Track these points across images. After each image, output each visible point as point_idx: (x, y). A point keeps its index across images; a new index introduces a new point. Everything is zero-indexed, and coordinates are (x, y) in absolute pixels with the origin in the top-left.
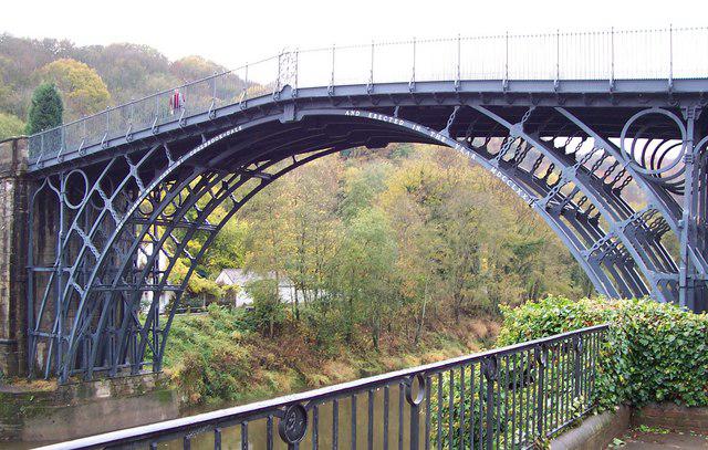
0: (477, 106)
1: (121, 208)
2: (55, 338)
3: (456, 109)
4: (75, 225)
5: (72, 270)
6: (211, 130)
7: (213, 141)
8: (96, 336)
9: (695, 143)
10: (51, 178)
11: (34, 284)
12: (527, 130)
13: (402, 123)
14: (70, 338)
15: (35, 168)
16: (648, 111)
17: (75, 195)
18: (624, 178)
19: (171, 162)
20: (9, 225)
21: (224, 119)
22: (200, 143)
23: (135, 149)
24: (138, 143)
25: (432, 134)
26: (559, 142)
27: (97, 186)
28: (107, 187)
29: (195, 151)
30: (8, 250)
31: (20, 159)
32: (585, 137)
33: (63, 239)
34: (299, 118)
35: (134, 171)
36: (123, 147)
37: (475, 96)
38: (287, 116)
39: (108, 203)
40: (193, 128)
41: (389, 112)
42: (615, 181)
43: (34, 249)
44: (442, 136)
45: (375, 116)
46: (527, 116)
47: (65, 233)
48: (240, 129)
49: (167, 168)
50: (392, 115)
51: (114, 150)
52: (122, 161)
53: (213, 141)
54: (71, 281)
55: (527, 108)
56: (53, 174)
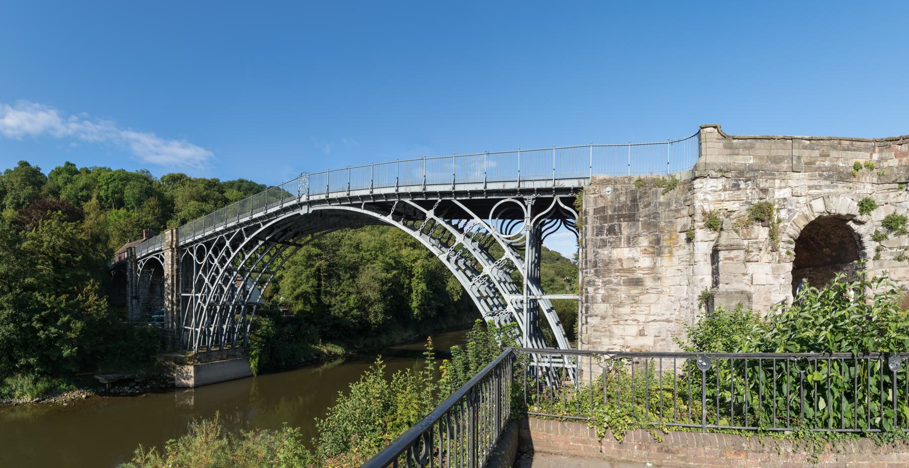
0: (407, 201)
1: (223, 261)
3: (396, 203)
4: (200, 273)
9: (531, 221)
11: (183, 303)
12: (437, 214)
13: (366, 212)
16: (502, 201)
18: (490, 242)
26: (455, 222)
32: (469, 218)
33: (195, 280)
37: (406, 195)
41: (359, 206)
42: (485, 243)
44: (388, 219)
45: (352, 209)
46: (436, 206)
50: (361, 208)
54: (199, 301)
55: (437, 201)
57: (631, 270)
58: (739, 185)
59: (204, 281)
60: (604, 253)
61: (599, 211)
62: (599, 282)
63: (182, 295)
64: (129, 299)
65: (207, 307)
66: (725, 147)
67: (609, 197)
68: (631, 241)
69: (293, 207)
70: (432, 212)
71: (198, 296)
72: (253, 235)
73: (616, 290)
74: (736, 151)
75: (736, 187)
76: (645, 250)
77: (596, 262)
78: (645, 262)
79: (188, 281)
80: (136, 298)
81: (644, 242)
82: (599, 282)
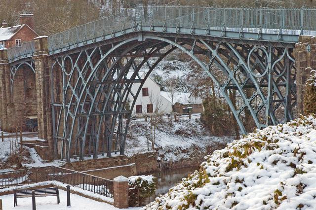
2: (64, 140)
4: (68, 84)
5: (69, 106)
6: (115, 42)
7: (117, 46)
8: (84, 139)
10: (58, 58)
14: (69, 140)
19: (102, 56)
20: (41, 84)
21: (116, 38)
22: (111, 48)
23: (90, 49)
25: (187, 52)
30: (42, 95)
31: (44, 49)
33: (64, 91)
34: (144, 40)
35: (89, 59)
36: (82, 47)
38: (140, 39)
39: (80, 73)
43: (54, 95)
47: (65, 88)
48: (125, 42)
49: (100, 59)
50: (174, 42)
51: (79, 48)
53: (117, 46)
56: (58, 57)
63: (55, 105)
65: (75, 118)
67: (309, 53)
69: (133, 34)
70: (215, 51)
71: (67, 107)
72: (107, 54)
79: (59, 90)
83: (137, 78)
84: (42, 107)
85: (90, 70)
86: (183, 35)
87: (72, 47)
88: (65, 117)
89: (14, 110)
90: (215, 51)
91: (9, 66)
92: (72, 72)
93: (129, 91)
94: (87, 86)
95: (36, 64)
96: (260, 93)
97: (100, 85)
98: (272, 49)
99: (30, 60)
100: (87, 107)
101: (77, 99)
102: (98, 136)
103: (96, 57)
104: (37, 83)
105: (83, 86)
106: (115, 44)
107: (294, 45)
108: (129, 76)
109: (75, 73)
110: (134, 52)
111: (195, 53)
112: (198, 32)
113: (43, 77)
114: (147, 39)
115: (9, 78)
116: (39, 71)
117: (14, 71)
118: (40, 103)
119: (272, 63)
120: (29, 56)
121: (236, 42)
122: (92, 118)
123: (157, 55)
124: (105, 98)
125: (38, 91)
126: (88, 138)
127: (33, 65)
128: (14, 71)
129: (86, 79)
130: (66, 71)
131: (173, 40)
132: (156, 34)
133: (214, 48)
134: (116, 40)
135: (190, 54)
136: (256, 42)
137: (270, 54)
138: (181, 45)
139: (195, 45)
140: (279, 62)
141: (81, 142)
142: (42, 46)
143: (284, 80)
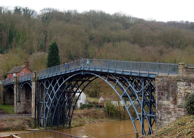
4: (47, 93)
5: (47, 103)
8: (53, 118)
14: (46, 118)
15: (39, 79)
17: (47, 85)
21: (72, 73)
23: (58, 77)
24: (58, 76)
25: (105, 80)
27: (51, 84)
28: (53, 84)
29: (68, 79)
35: (57, 81)
38: (82, 73)
39: (53, 88)
40: (67, 74)
47: (45, 94)
50: (99, 75)
52: (55, 78)
56: (43, 80)
57: (167, 109)
58: (190, 84)
59: (48, 96)
60: (160, 101)
61: (158, 87)
62: (159, 111)
64: (15, 102)
66: (186, 71)
68: (168, 98)
69: (79, 71)
72: (66, 80)
73: (164, 115)
74: (190, 73)
75: (190, 85)
76: (172, 102)
77: (158, 104)
78: (172, 106)
80: (19, 102)
81: (171, 99)
82: (159, 111)
83: (78, 91)
84: (34, 103)
85: (57, 87)
86: (103, 72)
87: (50, 76)
88: (45, 109)
89: (20, 104)
90: (118, 80)
91: (20, 84)
92: (49, 87)
93: (74, 97)
94: (55, 95)
95: (32, 83)
96: (139, 99)
97: (62, 94)
98: (144, 80)
99: (29, 81)
100: (55, 104)
101: (51, 100)
102: (59, 117)
103: (60, 82)
104: (32, 92)
105: (54, 95)
106: (70, 76)
107: (154, 79)
108: (75, 89)
109: (51, 88)
110: (78, 79)
111: (108, 80)
112: (110, 72)
113: (36, 90)
114: (86, 74)
115: (19, 89)
116: (33, 86)
117: (21, 86)
118: (34, 101)
119: (144, 87)
120: (29, 80)
121: (128, 77)
122: (57, 109)
123: (88, 81)
124: (63, 100)
125: (33, 96)
126: (54, 117)
127: (31, 84)
128: (21, 86)
129: (55, 91)
130: (46, 87)
131: (98, 74)
132: (90, 71)
133: (117, 79)
134: (71, 74)
135: (106, 81)
136: (137, 77)
137: (143, 82)
138: (101, 76)
139: (108, 77)
140: (146, 87)
141: (52, 119)
142: (35, 75)
143: (146, 94)
